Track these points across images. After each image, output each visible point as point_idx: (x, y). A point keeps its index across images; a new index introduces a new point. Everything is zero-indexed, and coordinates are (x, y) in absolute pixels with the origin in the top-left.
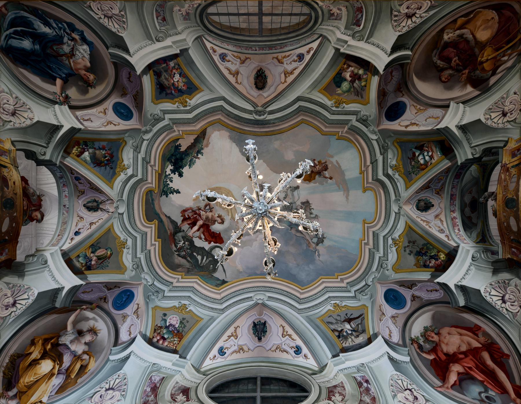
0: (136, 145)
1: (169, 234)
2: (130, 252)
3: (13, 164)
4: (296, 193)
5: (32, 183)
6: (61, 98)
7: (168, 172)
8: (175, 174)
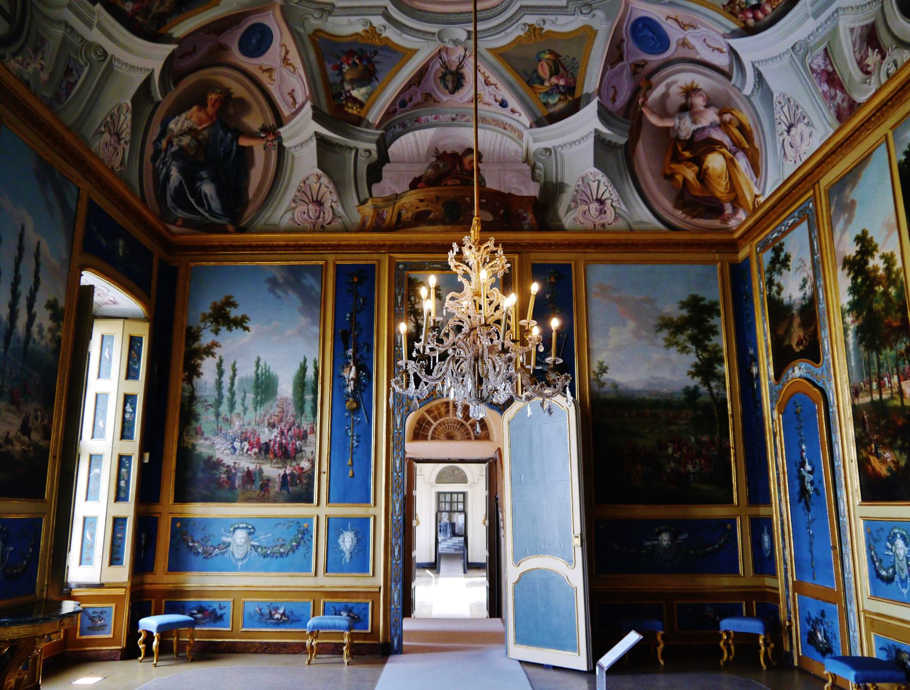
0: (318, 12)
2: (553, 18)
3: (392, 203)
5: (419, 170)
6: (270, 138)
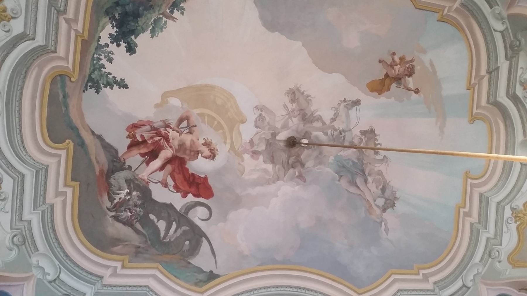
1: (97, 173)
4: (353, 112)
7: (105, 39)
8: (118, 45)
